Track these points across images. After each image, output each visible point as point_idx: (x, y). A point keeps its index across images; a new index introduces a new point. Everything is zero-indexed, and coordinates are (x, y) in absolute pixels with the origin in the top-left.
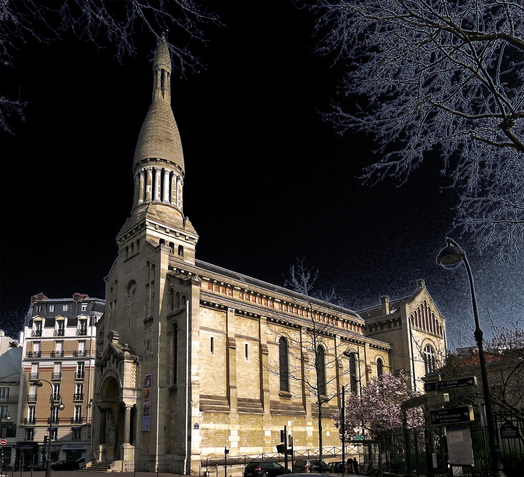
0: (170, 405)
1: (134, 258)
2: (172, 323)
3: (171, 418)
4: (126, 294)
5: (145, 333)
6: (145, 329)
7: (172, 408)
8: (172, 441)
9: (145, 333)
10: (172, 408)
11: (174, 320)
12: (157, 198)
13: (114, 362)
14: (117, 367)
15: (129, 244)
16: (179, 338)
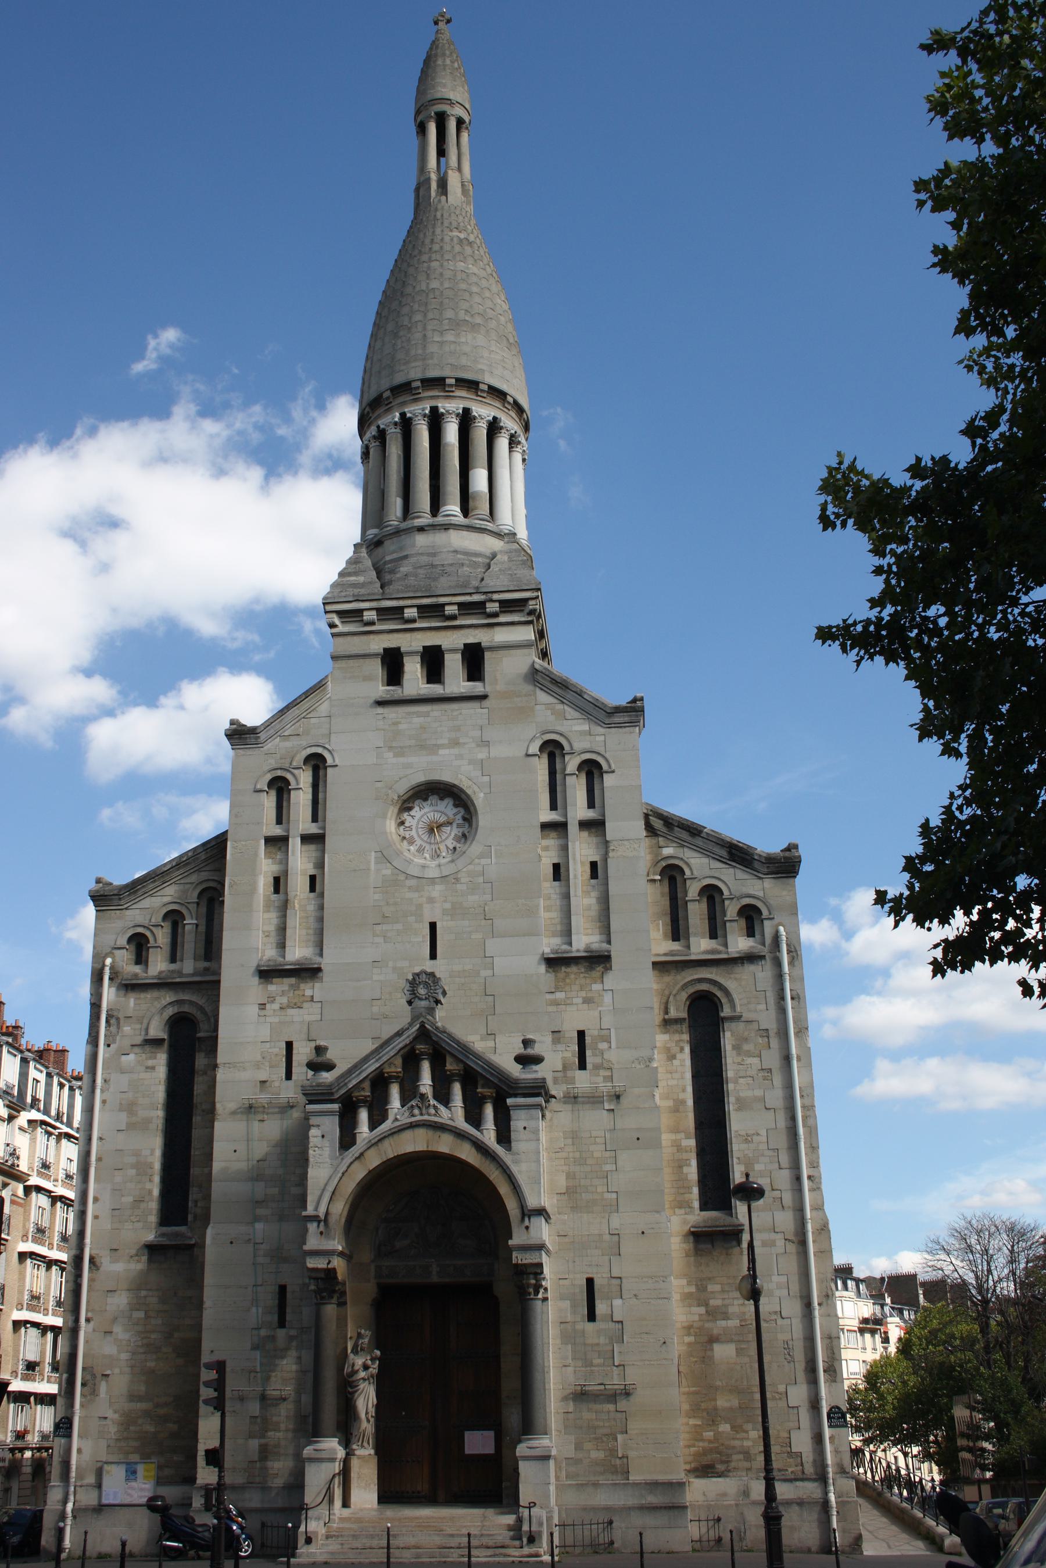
0: (702, 1288)
1: (455, 706)
2: (685, 986)
3: (713, 1340)
4: (391, 825)
5: (556, 1003)
6: (558, 989)
7: (712, 1302)
8: (725, 1428)
9: (556, 1003)
10: (712, 1302)
11: (700, 980)
12: (452, 508)
13: (443, 1096)
14: (474, 1118)
15: (412, 643)
16: (737, 1048)
